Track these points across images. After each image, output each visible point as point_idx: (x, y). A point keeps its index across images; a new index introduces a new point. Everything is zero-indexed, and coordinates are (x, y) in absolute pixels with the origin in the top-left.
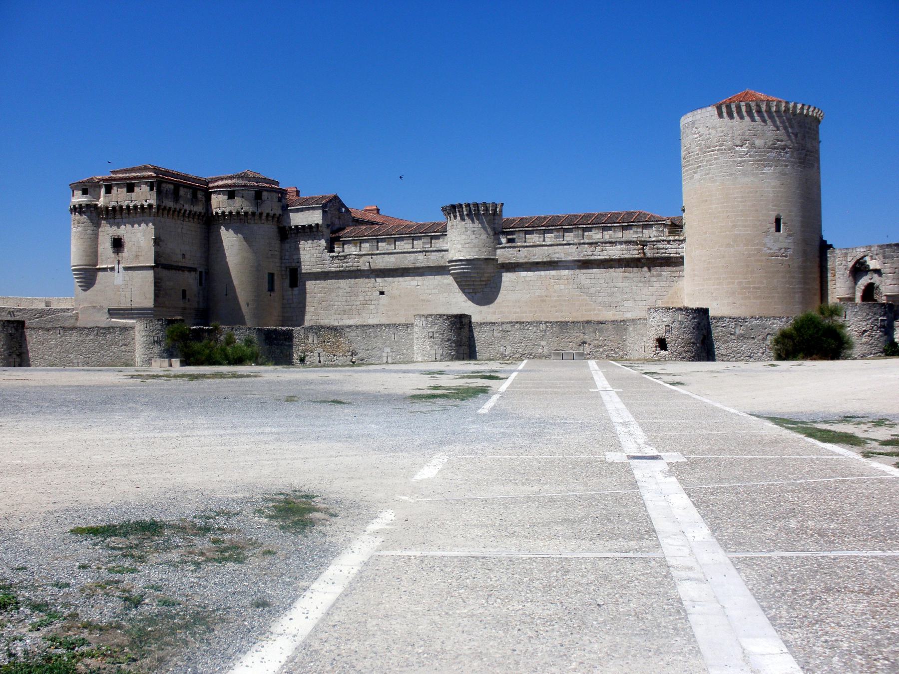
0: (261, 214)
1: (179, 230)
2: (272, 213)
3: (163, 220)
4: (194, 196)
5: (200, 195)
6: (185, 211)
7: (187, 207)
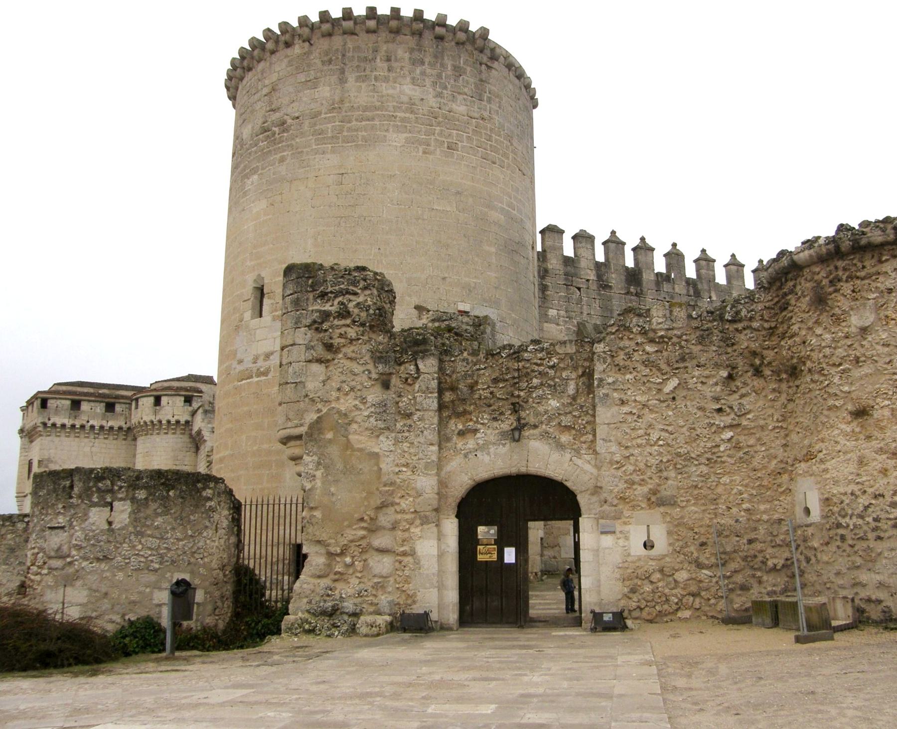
0: (160, 422)
1: (87, 449)
2: (173, 421)
3: (57, 440)
4: (110, 407)
5: (118, 408)
6: (92, 427)
7: (96, 423)
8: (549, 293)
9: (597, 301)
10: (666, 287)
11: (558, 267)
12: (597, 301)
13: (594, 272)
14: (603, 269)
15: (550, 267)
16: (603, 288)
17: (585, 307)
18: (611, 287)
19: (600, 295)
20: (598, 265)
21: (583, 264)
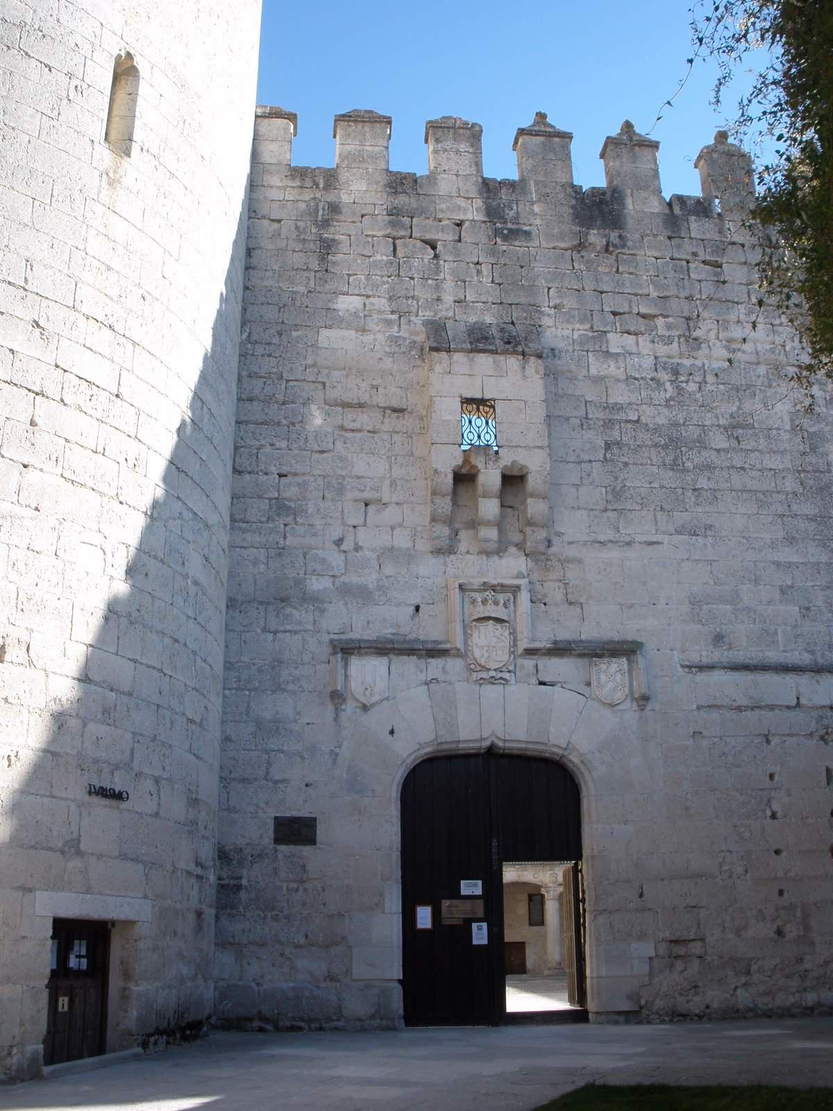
8: (340, 257)
9: (485, 269)
10: (697, 227)
11: (370, 198)
12: (485, 269)
13: (479, 203)
14: (504, 195)
15: (345, 198)
16: (505, 238)
17: (449, 285)
18: (527, 234)
19: (493, 252)
20: (489, 188)
21: (445, 185)
